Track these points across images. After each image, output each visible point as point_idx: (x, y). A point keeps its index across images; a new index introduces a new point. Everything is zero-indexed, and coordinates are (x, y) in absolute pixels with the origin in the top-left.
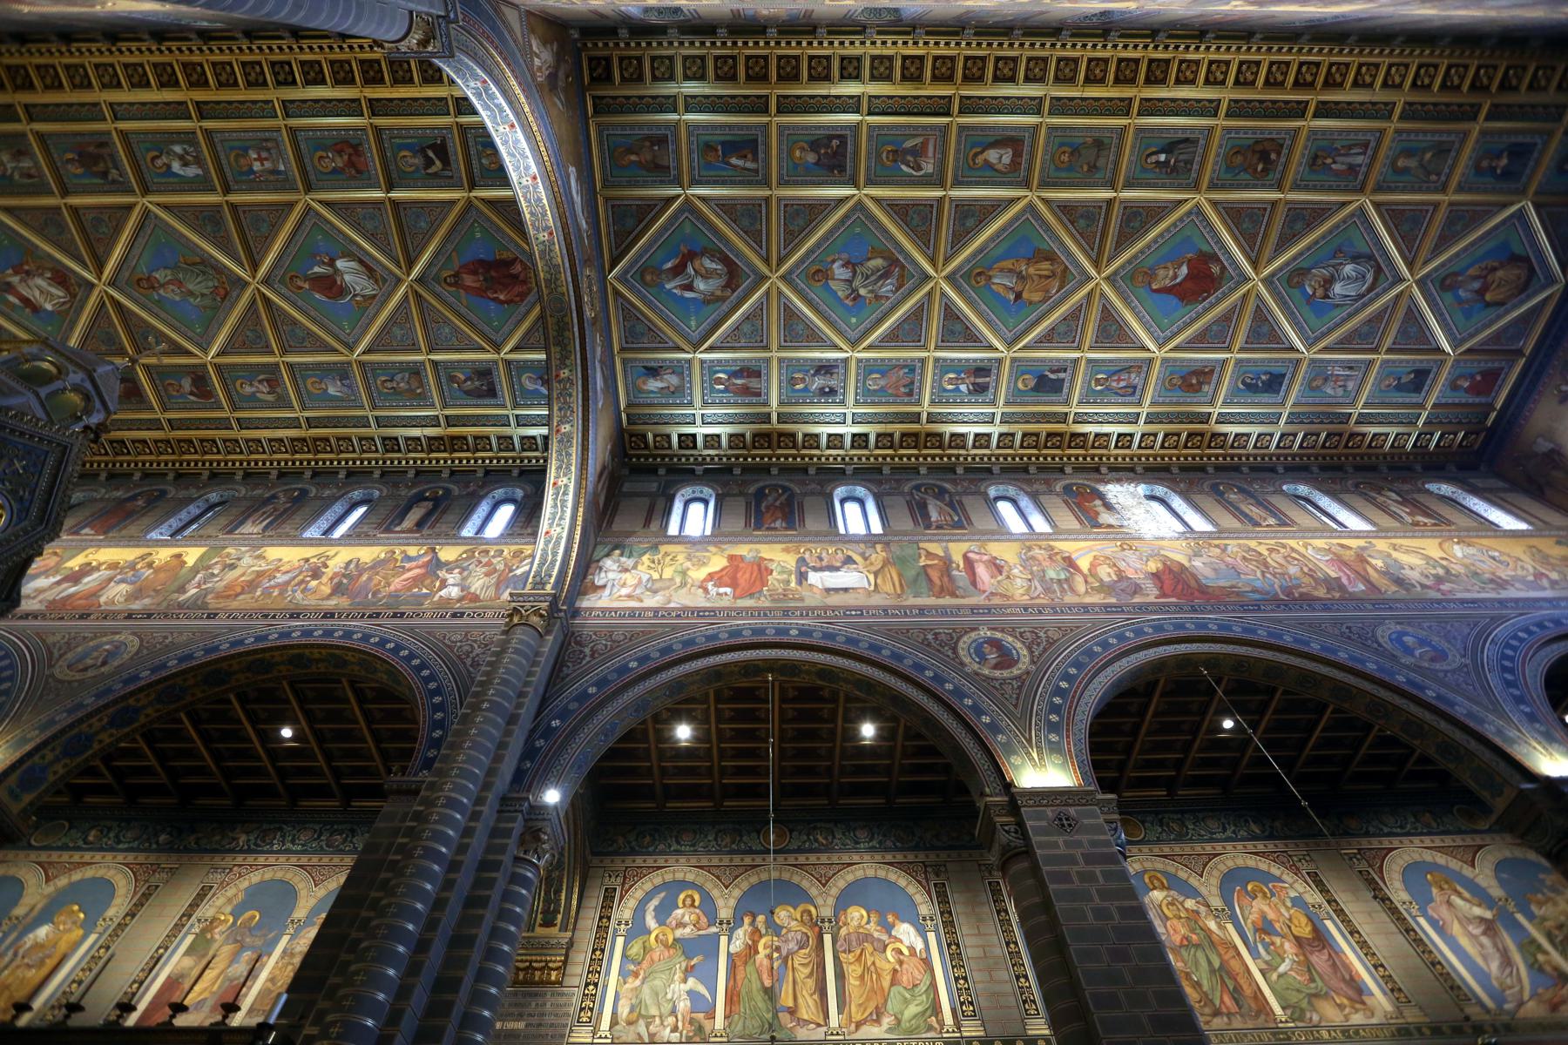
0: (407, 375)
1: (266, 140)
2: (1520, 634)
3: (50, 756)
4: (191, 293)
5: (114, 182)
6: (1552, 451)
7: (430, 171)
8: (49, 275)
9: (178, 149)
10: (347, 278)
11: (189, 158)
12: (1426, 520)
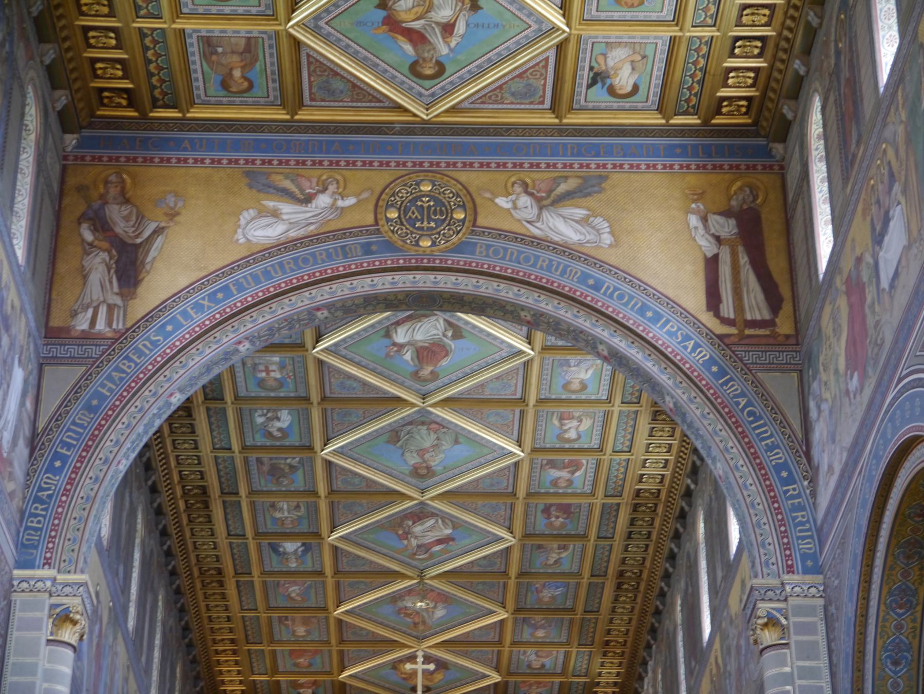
4: (436, 447)
8: (410, 523)
9: (260, 420)
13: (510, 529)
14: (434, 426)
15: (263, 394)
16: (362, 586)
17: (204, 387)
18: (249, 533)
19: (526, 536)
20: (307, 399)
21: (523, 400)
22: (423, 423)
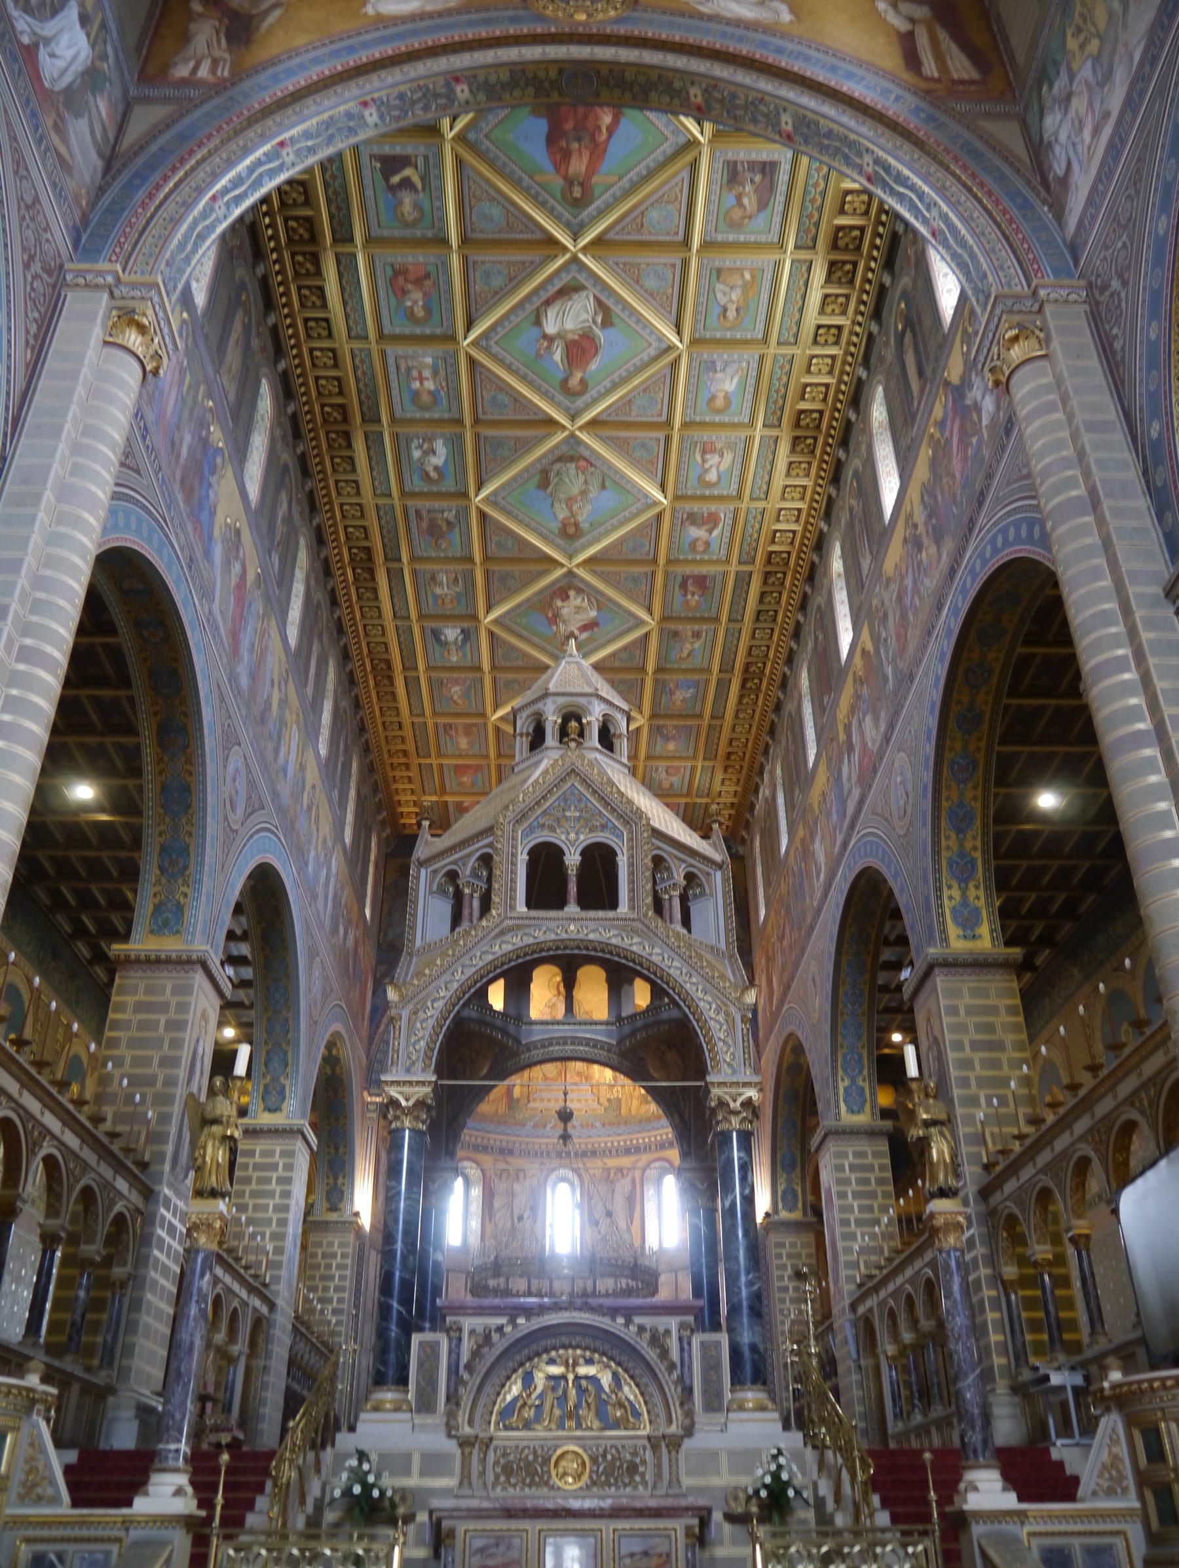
0: (719, 286)
1: (398, 368)
3: (956, 893)
4: (584, 493)
5: (457, 516)
7: (419, 186)
9: (417, 454)
10: (569, 325)
11: (425, 446)
13: (650, 610)
14: (582, 463)
15: (418, 415)
16: (516, 686)
17: (322, 165)
18: (413, 615)
19: (664, 619)
20: (460, 422)
21: (669, 423)
22: (571, 459)
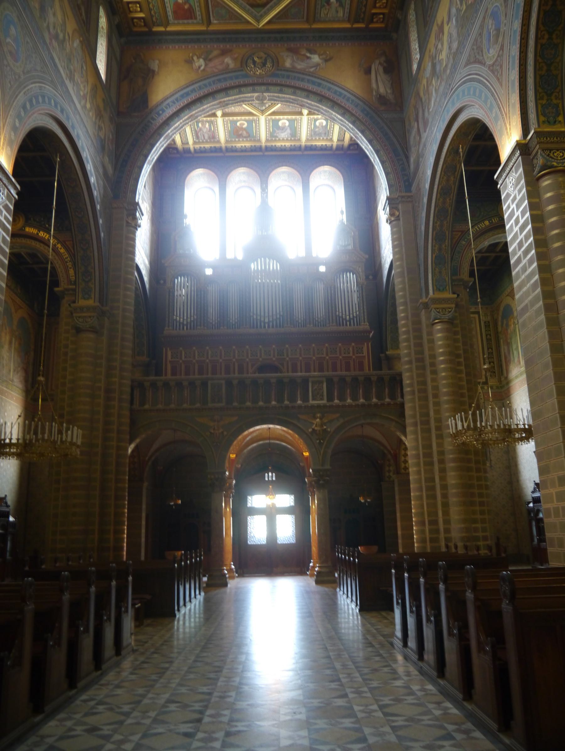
2: (53, 101)
6: (153, 72)
12: (83, 14)
